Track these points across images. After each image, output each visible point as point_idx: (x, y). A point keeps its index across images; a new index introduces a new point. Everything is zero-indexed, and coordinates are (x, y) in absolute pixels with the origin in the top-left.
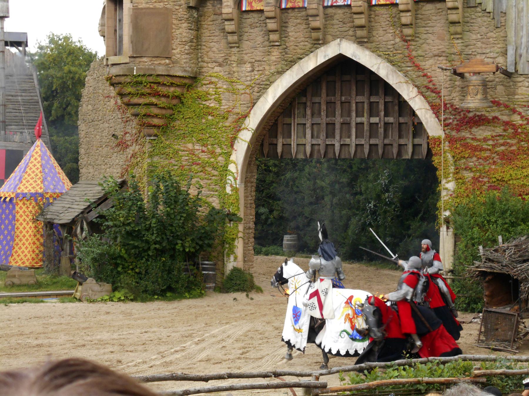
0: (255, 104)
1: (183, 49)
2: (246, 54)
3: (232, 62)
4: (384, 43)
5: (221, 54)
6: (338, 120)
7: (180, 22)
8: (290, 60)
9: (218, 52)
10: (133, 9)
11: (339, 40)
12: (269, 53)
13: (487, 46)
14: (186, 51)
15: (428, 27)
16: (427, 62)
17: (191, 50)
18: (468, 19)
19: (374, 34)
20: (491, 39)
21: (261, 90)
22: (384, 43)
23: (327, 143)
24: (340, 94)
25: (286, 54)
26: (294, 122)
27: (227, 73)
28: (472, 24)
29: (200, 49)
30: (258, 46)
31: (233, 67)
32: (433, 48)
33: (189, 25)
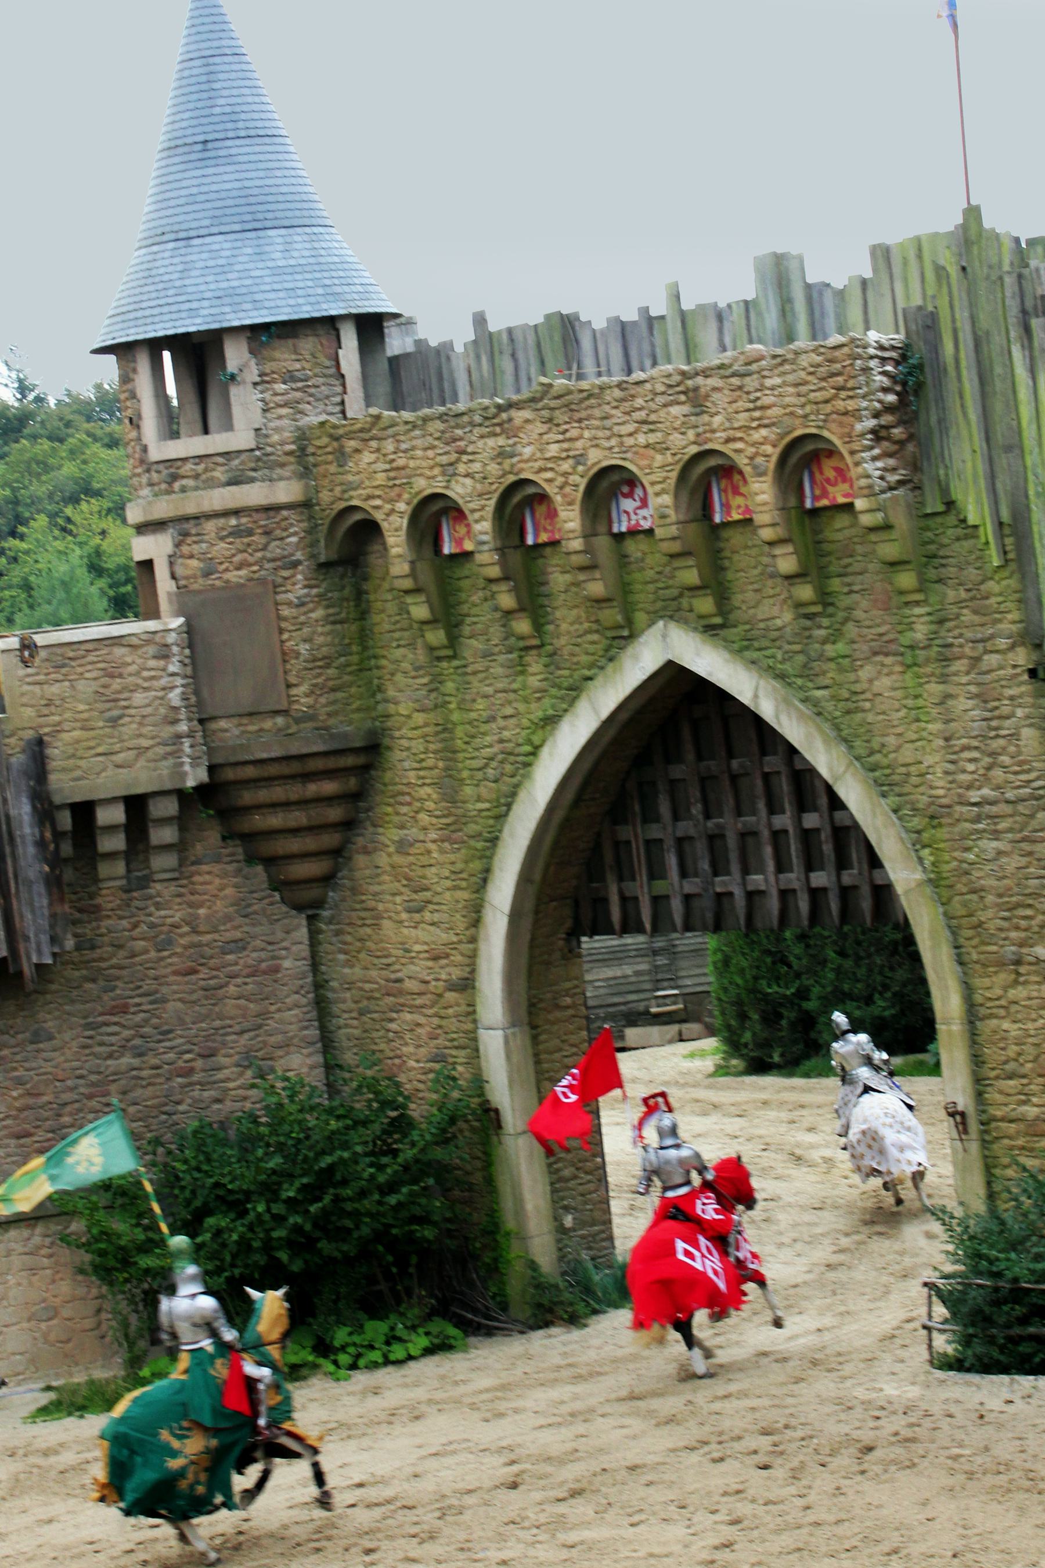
0: (509, 806)
1: (320, 680)
2: (475, 673)
3: (447, 699)
4: (762, 625)
5: (422, 676)
6: (730, 824)
7: (303, 609)
8: (565, 684)
9: (413, 674)
10: (178, 595)
11: (661, 623)
12: (520, 668)
13: (984, 619)
14: (331, 683)
15: (852, 574)
16: (860, 673)
17: (346, 678)
18: (932, 547)
19: (737, 604)
20: (993, 600)
21: (518, 769)
22: (762, 625)
23: (718, 890)
24: (723, 754)
25: (559, 669)
26: (636, 836)
27: (440, 728)
28: (943, 561)
29: (378, 667)
30: (497, 649)
31: (451, 711)
32: (866, 630)
33: (331, 611)
